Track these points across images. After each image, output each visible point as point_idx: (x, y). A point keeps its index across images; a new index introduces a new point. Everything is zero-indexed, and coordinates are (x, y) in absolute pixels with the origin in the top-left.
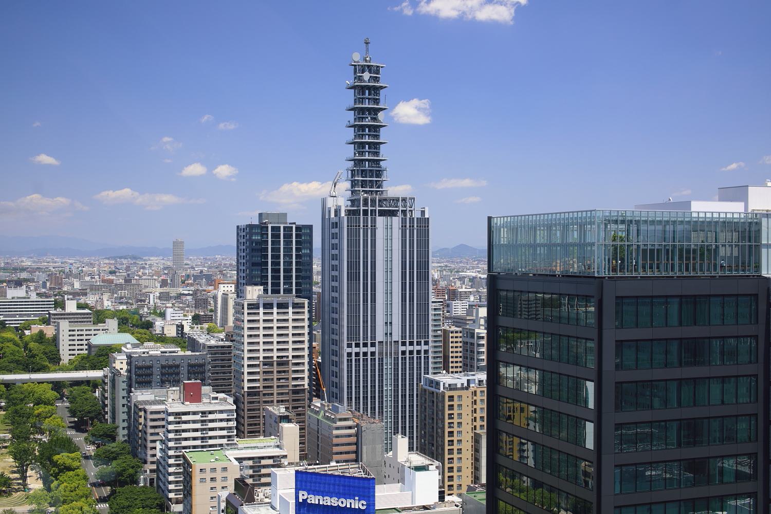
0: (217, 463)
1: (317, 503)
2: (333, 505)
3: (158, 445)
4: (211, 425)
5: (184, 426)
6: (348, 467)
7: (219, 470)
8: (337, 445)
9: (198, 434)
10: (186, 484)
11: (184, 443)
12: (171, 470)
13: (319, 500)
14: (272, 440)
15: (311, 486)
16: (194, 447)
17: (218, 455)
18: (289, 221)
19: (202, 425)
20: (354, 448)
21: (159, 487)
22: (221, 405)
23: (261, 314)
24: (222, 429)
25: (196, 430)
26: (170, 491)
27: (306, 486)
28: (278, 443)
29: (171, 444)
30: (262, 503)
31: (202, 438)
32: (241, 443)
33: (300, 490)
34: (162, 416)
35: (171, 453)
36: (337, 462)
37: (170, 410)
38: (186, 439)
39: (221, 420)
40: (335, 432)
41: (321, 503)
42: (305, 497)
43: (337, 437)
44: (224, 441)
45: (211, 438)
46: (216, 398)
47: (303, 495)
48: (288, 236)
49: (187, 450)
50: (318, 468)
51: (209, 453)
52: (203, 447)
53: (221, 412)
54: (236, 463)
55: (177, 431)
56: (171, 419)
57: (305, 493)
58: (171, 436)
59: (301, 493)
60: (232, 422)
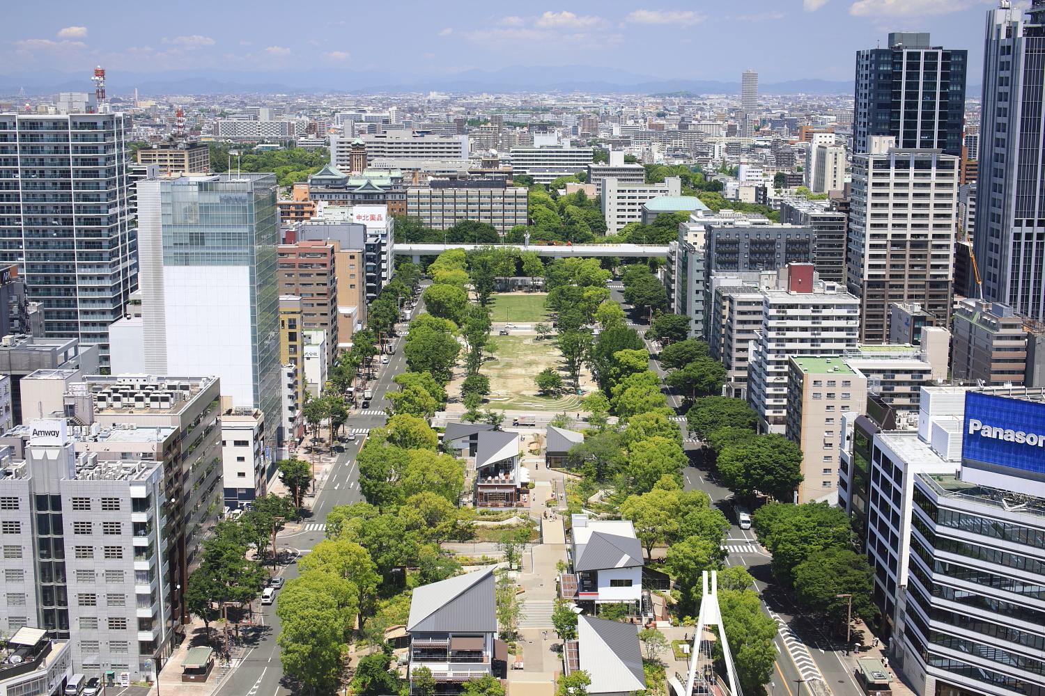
0: (836, 374)
1: (995, 436)
2: (1018, 441)
3: (752, 346)
4: (825, 324)
5: (789, 323)
6: (1023, 392)
7: (839, 383)
8: (998, 361)
9: (807, 335)
10: (792, 400)
11: (789, 346)
12: (770, 379)
13: (998, 433)
14: (907, 349)
15: (987, 414)
16: (802, 351)
17: (837, 363)
18: (932, 44)
19: (813, 323)
20: (1022, 366)
21: (750, 400)
22: (839, 297)
23: (912, 175)
24: (839, 329)
25: (804, 329)
26: (767, 407)
27: (980, 413)
28: (919, 353)
29: (771, 346)
30: (905, 432)
31: (813, 340)
32: (866, 349)
33: (971, 417)
34: (760, 308)
35: (771, 357)
36: (1014, 384)
37: (772, 301)
38: (791, 340)
39: (839, 318)
40: (996, 343)
41: (1001, 437)
42: (978, 428)
43: (999, 349)
44: (842, 346)
45: (824, 340)
46: (833, 288)
47: (975, 425)
48: (930, 66)
49: (795, 355)
50: (997, 390)
51: (825, 360)
52: (812, 352)
53: (839, 306)
54: (862, 376)
55: (779, 329)
56: (772, 312)
57: (979, 422)
58: (772, 335)
59: (972, 422)
60: (854, 322)
